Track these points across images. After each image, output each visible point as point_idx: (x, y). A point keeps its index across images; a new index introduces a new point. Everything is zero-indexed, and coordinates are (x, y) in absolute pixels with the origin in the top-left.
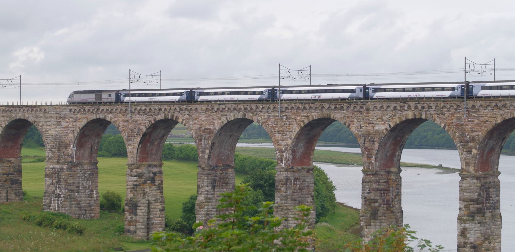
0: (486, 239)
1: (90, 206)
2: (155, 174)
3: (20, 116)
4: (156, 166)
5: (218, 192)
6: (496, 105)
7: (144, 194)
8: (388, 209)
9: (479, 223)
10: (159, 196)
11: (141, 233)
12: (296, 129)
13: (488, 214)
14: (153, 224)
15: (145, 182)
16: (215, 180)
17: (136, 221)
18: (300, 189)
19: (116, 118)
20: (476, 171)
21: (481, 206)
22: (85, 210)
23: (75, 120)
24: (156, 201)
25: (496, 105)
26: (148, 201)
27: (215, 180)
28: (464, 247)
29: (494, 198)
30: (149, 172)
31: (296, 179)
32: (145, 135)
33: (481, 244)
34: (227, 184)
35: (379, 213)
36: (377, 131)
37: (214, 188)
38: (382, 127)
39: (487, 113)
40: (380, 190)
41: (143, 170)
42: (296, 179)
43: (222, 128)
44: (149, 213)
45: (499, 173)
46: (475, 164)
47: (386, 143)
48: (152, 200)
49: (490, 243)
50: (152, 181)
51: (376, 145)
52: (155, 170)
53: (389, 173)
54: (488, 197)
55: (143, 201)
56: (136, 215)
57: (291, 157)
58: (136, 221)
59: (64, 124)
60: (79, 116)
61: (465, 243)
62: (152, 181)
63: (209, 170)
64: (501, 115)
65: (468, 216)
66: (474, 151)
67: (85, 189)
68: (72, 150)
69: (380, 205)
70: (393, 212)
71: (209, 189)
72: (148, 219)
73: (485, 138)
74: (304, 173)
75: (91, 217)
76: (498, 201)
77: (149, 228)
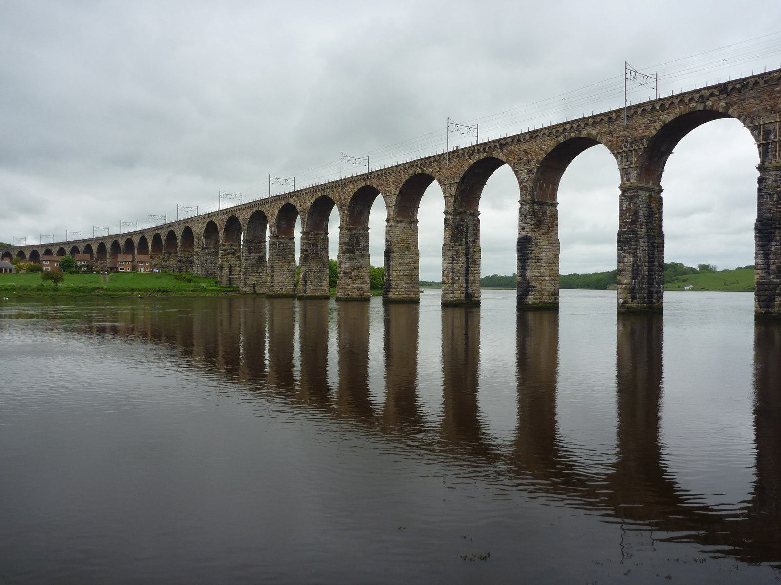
0: (354, 269)
1: (215, 271)
2: (235, 250)
3: (187, 225)
4: (236, 246)
5: (252, 256)
6: (354, 180)
7: (228, 261)
8: (316, 256)
9: (348, 258)
10: (238, 263)
11: (225, 283)
12: (277, 212)
13: (357, 253)
14: (233, 278)
15: (228, 254)
16: (250, 249)
17: (222, 276)
18: (283, 249)
19: (215, 220)
20: (349, 225)
21: (351, 247)
22: (211, 274)
23: (203, 223)
24: (236, 265)
25: (354, 180)
26: (230, 265)
27: (250, 249)
28: (340, 274)
29: (363, 243)
30: (231, 249)
31: (280, 243)
32: (226, 227)
33: (350, 273)
34: (260, 252)
35: (309, 258)
36: (307, 207)
37: (250, 253)
38: (309, 205)
39: (351, 186)
40: (310, 244)
41: (227, 247)
42: (280, 243)
43: (251, 217)
44: (231, 271)
45: (369, 228)
46: (346, 219)
47: (313, 215)
48: (232, 264)
49: (359, 272)
50: (234, 254)
51: (307, 215)
52: (235, 248)
53: (318, 234)
54: (358, 243)
55: (227, 264)
56: (222, 272)
57: (276, 230)
58: (222, 276)
59: (200, 226)
60: (205, 221)
61: (341, 271)
62: (234, 254)
63: (247, 243)
64: (357, 186)
65: (342, 254)
66: (346, 212)
67: (211, 262)
68: (203, 240)
69: (310, 253)
70: (320, 258)
71: (247, 253)
72: (230, 275)
73: (351, 202)
74: (287, 240)
75: (215, 277)
76: (368, 246)
77: (230, 280)
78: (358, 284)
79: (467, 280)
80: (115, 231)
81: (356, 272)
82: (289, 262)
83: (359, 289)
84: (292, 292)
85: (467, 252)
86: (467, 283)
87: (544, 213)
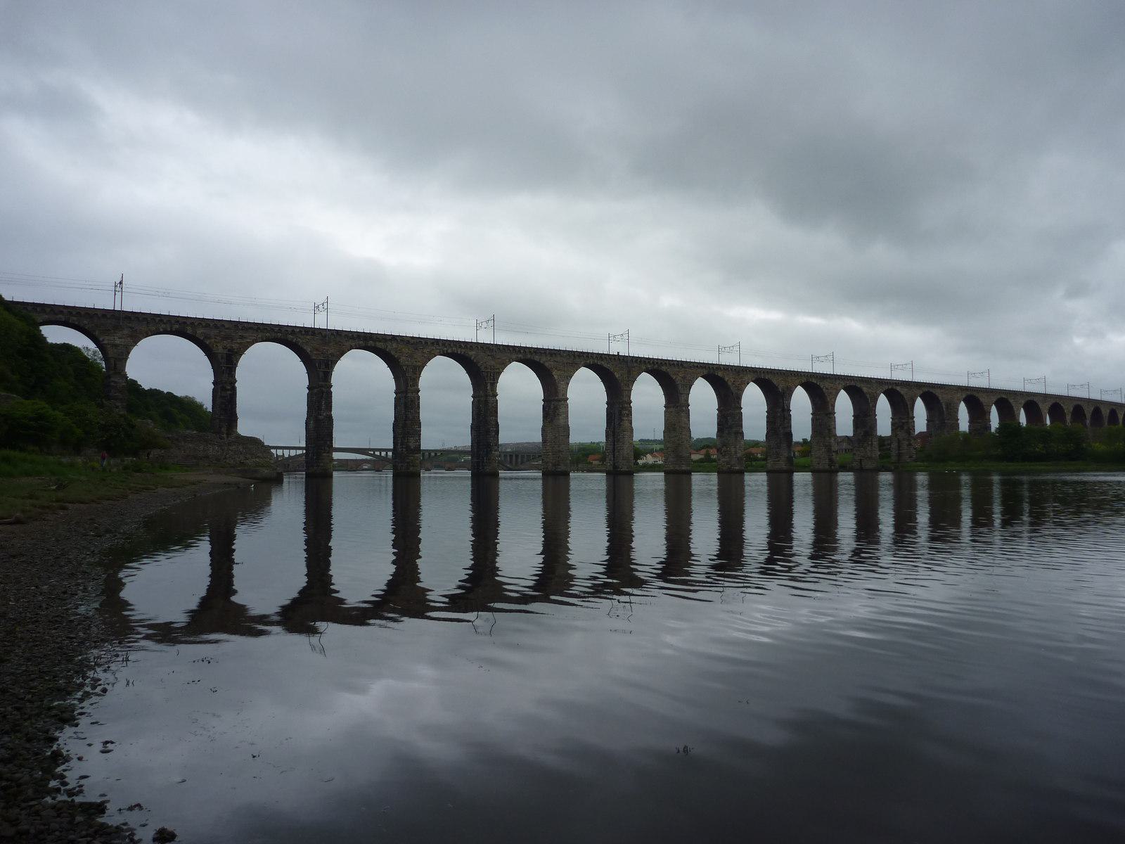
2: (903, 423)
24: (904, 439)
44: (899, 447)
52: (903, 421)
72: (899, 450)
77: (899, 455)
78: (726, 459)
79: (614, 455)
80: (1095, 396)
81: (724, 448)
82: (824, 437)
83: (728, 463)
84: (827, 467)
85: (614, 432)
86: (614, 457)
87: (550, 407)
